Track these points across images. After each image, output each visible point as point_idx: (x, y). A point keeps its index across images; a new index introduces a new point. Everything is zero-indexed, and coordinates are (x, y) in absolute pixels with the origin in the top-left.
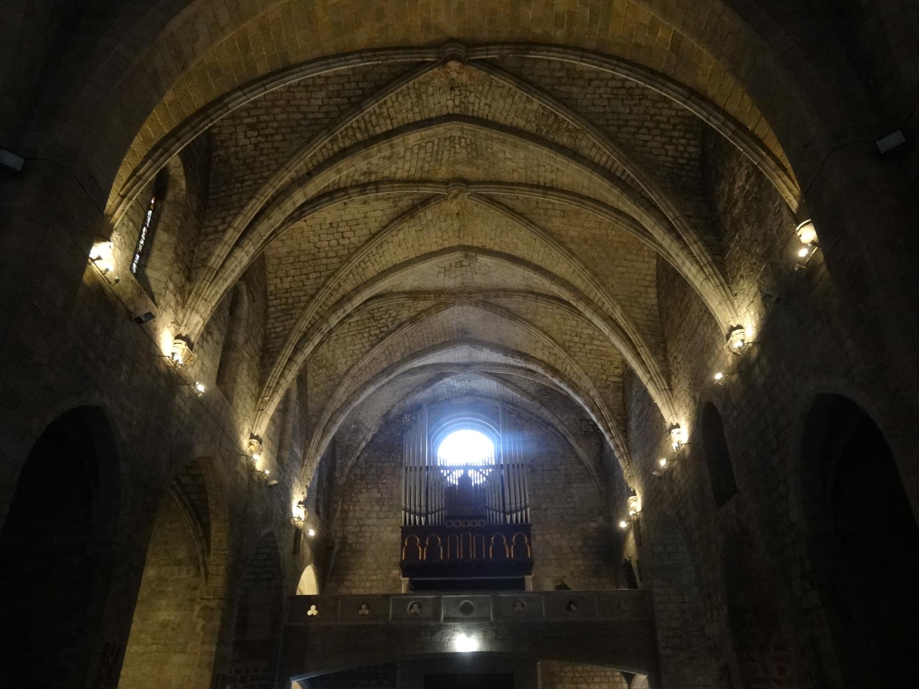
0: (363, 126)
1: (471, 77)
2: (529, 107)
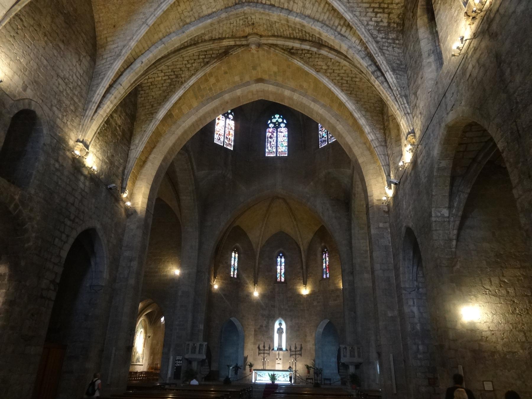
0: (304, 33)
1: (244, 31)
2: (210, 35)
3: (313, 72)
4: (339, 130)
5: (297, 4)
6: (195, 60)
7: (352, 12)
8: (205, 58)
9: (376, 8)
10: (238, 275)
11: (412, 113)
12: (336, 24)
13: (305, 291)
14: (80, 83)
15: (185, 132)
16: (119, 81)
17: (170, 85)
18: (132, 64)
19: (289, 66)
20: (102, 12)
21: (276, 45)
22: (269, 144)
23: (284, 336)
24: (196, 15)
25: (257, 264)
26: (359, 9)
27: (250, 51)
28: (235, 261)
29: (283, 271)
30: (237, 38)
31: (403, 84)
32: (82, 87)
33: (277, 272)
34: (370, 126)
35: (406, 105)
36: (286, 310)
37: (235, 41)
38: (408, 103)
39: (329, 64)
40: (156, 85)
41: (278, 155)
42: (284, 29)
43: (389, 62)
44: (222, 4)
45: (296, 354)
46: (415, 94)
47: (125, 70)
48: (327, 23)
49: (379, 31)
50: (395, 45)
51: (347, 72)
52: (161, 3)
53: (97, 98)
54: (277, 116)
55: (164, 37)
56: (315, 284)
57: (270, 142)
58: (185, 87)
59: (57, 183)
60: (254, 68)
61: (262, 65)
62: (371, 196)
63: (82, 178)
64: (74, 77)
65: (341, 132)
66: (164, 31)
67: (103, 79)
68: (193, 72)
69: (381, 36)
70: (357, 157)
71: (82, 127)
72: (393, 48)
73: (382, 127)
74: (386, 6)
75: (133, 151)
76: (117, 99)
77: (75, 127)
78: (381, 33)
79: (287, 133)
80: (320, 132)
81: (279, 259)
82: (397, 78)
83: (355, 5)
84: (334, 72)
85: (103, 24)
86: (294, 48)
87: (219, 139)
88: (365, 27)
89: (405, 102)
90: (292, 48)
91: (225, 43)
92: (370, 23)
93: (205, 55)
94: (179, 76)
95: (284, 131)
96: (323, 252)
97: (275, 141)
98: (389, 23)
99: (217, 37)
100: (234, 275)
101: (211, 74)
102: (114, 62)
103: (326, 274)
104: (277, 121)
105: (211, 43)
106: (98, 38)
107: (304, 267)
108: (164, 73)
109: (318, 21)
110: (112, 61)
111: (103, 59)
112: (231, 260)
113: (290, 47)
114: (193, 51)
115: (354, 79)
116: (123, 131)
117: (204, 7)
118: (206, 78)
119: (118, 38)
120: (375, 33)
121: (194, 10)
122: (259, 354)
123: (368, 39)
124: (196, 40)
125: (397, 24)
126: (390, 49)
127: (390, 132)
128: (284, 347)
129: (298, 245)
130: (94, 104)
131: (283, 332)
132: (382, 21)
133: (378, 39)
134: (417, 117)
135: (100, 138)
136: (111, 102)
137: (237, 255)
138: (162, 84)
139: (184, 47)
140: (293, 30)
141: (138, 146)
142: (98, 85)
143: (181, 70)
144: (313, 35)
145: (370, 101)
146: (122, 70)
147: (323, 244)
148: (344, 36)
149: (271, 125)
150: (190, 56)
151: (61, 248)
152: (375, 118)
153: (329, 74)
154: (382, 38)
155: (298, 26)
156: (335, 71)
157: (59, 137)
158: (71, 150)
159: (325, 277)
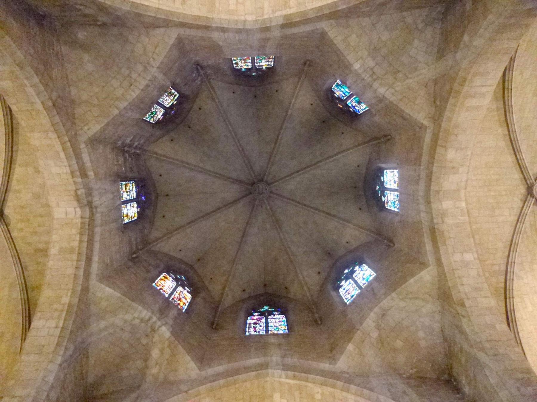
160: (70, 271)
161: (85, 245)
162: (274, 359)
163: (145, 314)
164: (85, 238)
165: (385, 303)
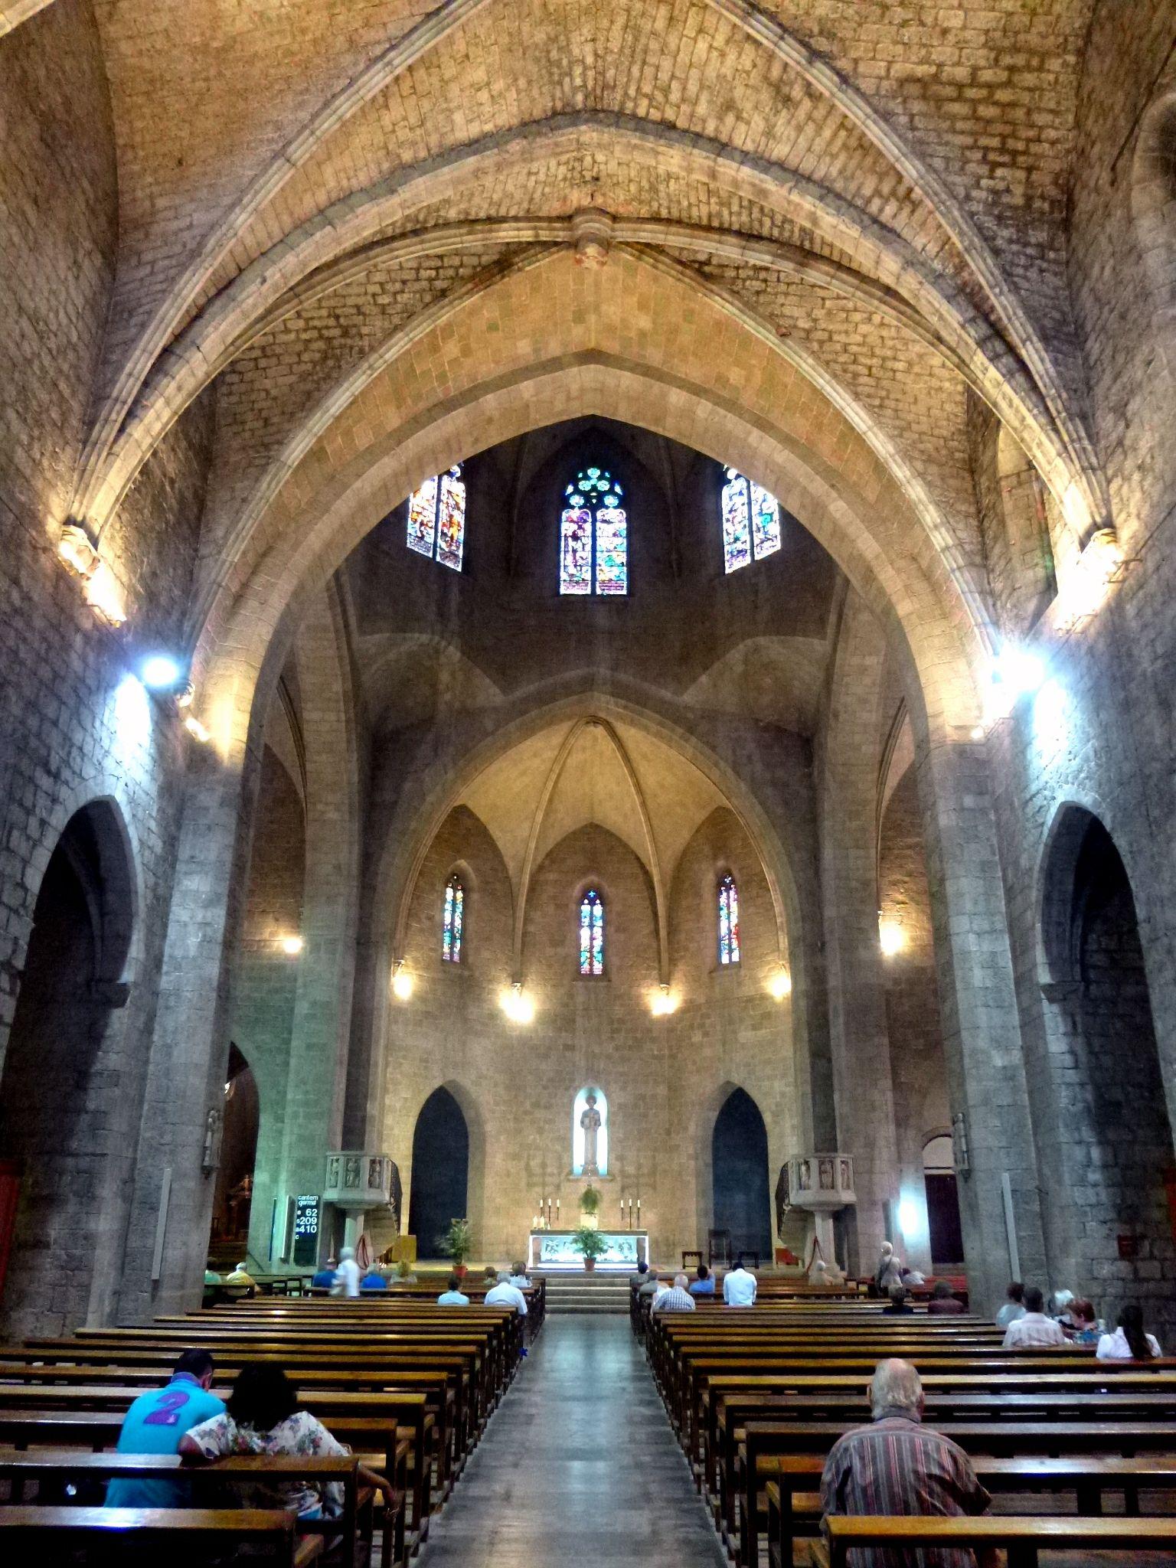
0: (756, 214)
1: (565, 199)
3: (768, 337)
4: (837, 515)
5: (748, 123)
6: (404, 282)
7: (922, 156)
8: (437, 278)
9: (994, 149)
10: (463, 952)
11: (1104, 468)
12: (867, 191)
13: (663, 1001)
14: (75, 339)
15: (362, 507)
16: (192, 334)
17: (325, 358)
18: (230, 283)
19: (689, 315)
20: (143, 117)
21: (659, 249)
22: (570, 557)
23: (602, 1133)
24: (434, 140)
25: (520, 925)
26: (941, 150)
27: (579, 262)
28: (454, 911)
29: (598, 944)
30: (540, 219)
31: (1073, 380)
32: (81, 347)
33: (579, 946)
34: (937, 504)
35: (1086, 442)
36: (609, 1057)
37: (535, 228)
38: (1090, 437)
39: (819, 313)
40: (278, 356)
41: (599, 592)
42: (693, 200)
43: (1031, 313)
44: (515, 110)
45: (637, 1185)
46: (1120, 410)
47: (210, 301)
48: (839, 186)
49: (1000, 219)
50: (1045, 265)
51: (869, 340)
52: (334, 96)
53: (127, 386)
54: (593, 473)
55: (332, 204)
56: (694, 981)
57: (575, 551)
58: (370, 367)
59: (16, 653)
60: (579, 317)
61: (604, 307)
62: (935, 716)
63: (78, 640)
64: (62, 314)
65: (842, 522)
66: (332, 184)
67: (143, 326)
68: (396, 320)
69: (1006, 233)
70: (894, 599)
71: (81, 478)
72: (1042, 271)
73: (972, 510)
74: (1020, 146)
75: (210, 561)
76: (184, 393)
77: (62, 478)
78: (1007, 227)
79: (624, 525)
80: (726, 526)
81: (586, 909)
82: (1056, 363)
83: (932, 137)
84: (830, 339)
85: (141, 153)
86: (714, 261)
87: (422, 538)
88: (961, 203)
89: (1083, 434)
90: (708, 263)
91: (508, 234)
92: (975, 193)
93: (437, 269)
94: (354, 331)
95: (614, 520)
96: (720, 885)
97: (588, 548)
98: (1029, 199)
99: (482, 215)
100: (452, 953)
101: (448, 331)
102: (181, 274)
103: (731, 951)
104: (594, 488)
105: (464, 231)
106: (125, 199)
107: (663, 933)
108: (307, 320)
109: (809, 179)
110: (173, 272)
111: (140, 264)
112: (443, 910)
113: (702, 257)
114: (407, 253)
115: (889, 364)
116: (182, 500)
117: (458, 117)
118: (432, 344)
119: (192, 200)
120: (989, 223)
121: (429, 125)
122: (530, 1185)
123: (971, 242)
124: (421, 217)
125: (1052, 203)
126: (1033, 274)
127: (1002, 523)
128: (602, 1165)
129: (642, 866)
130: (118, 407)
131: (597, 1123)
132: (1008, 190)
133: (999, 242)
134: (1127, 479)
135: (125, 516)
136: (168, 403)
137: (460, 895)
138: (299, 355)
139: (385, 240)
140: (721, 204)
141: (224, 545)
142: (129, 344)
143: (360, 313)
144: (785, 220)
145: (936, 432)
146: (202, 301)
147: (721, 863)
148: (891, 230)
149: (576, 500)
150: (389, 272)
151: (26, 862)
152: (952, 482)
153: (815, 346)
154: (1011, 241)
155: (746, 193)
156: (836, 337)
157: (22, 505)
158: (48, 549)
159: (725, 960)
160: (331, 652)
161: (339, 618)
162: (602, 670)
163: (424, 638)
164: (339, 610)
165: (762, 640)
